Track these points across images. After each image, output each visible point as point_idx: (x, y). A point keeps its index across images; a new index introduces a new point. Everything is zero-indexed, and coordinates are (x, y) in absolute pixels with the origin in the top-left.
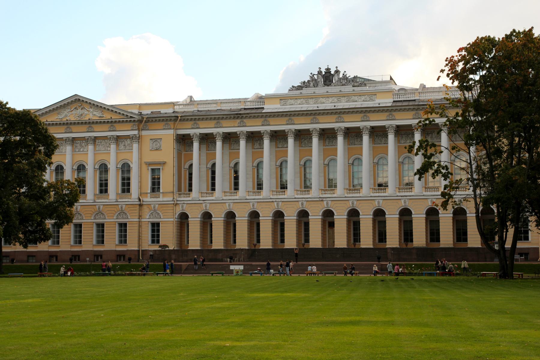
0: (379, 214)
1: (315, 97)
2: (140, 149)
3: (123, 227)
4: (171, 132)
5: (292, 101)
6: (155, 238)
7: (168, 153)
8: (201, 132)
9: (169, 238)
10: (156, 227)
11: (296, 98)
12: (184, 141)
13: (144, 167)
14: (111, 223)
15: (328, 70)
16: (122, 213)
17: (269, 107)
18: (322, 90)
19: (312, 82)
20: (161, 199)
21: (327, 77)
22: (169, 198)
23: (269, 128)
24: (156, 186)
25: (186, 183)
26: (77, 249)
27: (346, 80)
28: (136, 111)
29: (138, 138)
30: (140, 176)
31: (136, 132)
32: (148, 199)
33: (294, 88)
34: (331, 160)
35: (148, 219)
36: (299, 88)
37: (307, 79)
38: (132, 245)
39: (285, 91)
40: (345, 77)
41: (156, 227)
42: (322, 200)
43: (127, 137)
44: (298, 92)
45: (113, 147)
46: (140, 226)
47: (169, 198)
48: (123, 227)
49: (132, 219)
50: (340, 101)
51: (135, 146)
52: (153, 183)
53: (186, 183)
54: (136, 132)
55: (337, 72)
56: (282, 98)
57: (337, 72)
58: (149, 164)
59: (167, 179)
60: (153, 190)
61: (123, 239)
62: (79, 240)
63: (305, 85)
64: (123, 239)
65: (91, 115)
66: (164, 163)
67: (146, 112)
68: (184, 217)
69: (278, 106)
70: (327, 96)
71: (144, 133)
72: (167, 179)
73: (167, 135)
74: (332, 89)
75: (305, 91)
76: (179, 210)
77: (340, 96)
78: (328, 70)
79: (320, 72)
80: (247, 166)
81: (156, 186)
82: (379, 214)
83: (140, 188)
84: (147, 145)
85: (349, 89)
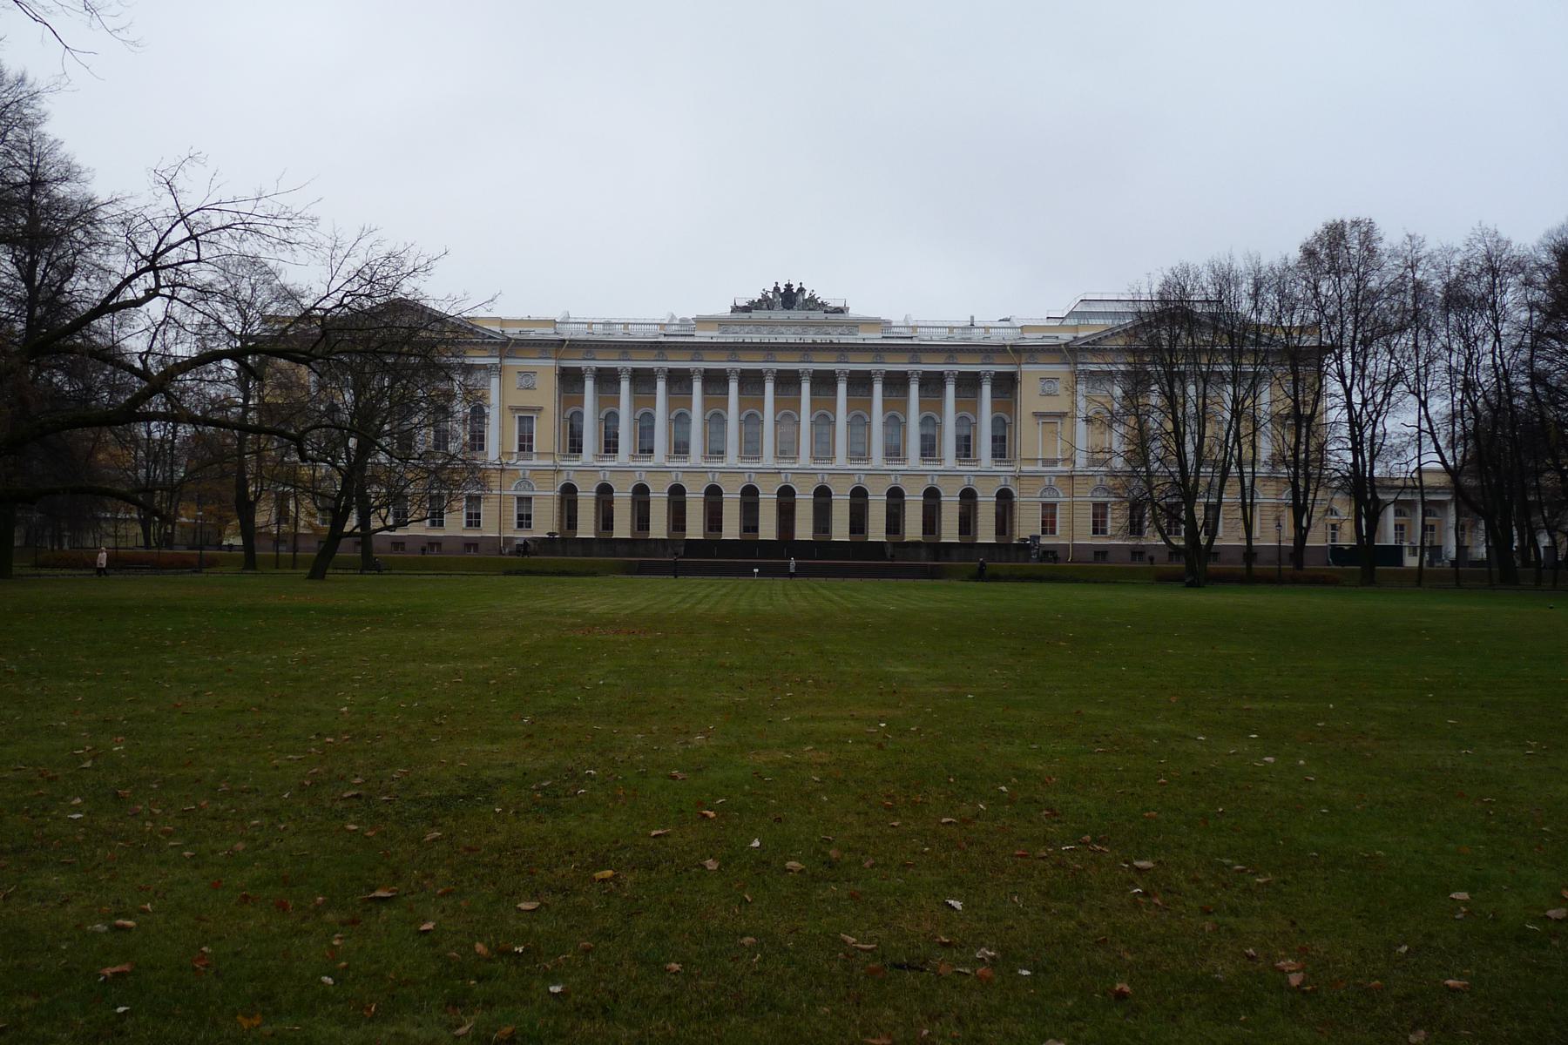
0: (859, 494)
1: (771, 324)
4: (552, 363)
5: (737, 329)
6: (524, 521)
7: (546, 393)
8: (593, 368)
11: (742, 324)
12: (570, 380)
13: (508, 412)
15: (789, 286)
17: (703, 336)
18: (780, 315)
19: (764, 303)
20: (535, 462)
21: (789, 297)
24: (526, 444)
26: (472, 534)
27: (813, 304)
28: (497, 329)
29: (499, 370)
30: (502, 427)
31: (496, 361)
33: (735, 309)
34: (680, 414)
35: (512, 491)
36: (746, 309)
37: (757, 296)
39: (724, 310)
40: (812, 299)
42: (779, 472)
43: (484, 367)
44: (746, 315)
50: (805, 333)
51: (495, 382)
52: (521, 439)
54: (496, 361)
55: (801, 290)
56: (720, 323)
57: (801, 290)
58: (518, 409)
60: (521, 448)
61: (1048, 525)
62: (474, 520)
66: (540, 409)
67: (512, 332)
68: (569, 491)
69: (715, 334)
70: (789, 324)
71: (508, 362)
72: (546, 433)
73: (546, 368)
74: (796, 315)
75: (755, 315)
76: (562, 480)
77: (807, 325)
78: (789, 286)
79: (777, 289)
81: (526, 444)
82: (859, 494)
83: (502, 444)
84: (514, 380)
85: (818, 315)
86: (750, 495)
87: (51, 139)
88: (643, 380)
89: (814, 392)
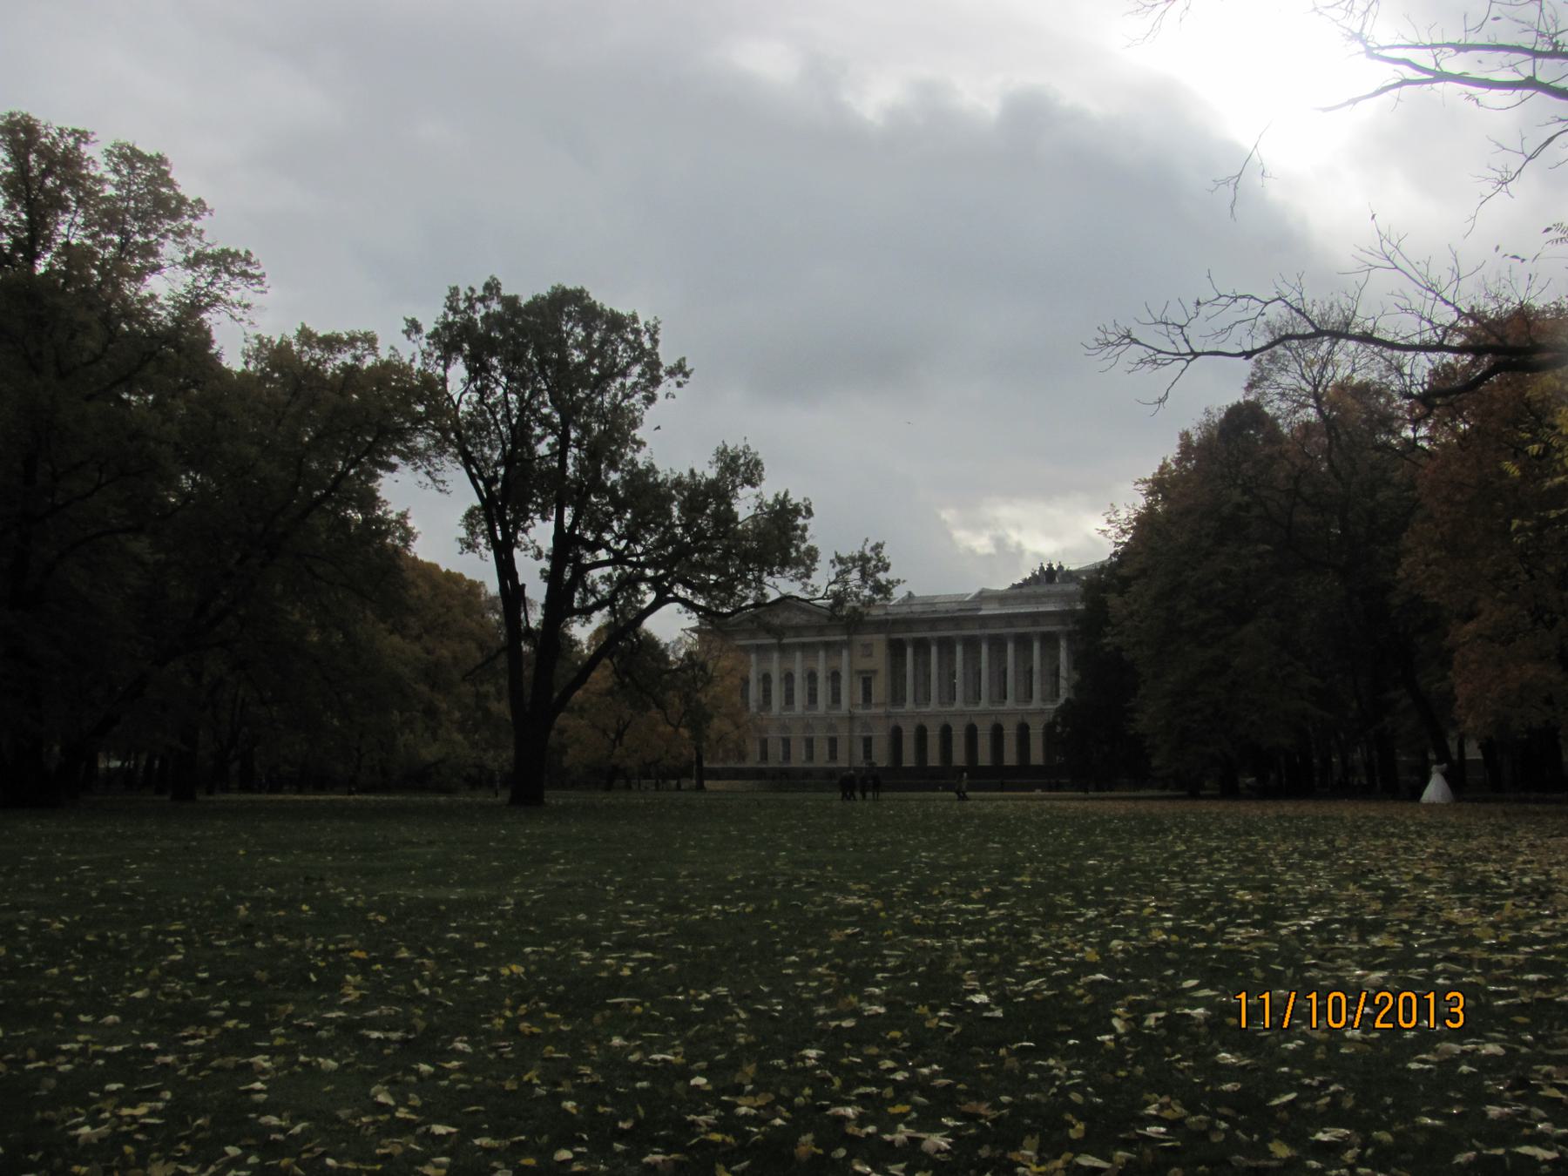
2: (850, 655)
3: (833, 742)
4: (882, 636)
7: (879, 660)
9: (881, 759)
10: (868, 742)
12: (897, 648)
14: (820, 735)
16: (831, 727)
17: (987, 610)
18: (1042, 589)
22: (880, 711)
23: (1013, 630)
25: (897, 697)
29: (847, 644)
32: (859, 711)
35: (858, 732)
36: (1020, 586)
38: (842, 762)
41: (868, 742)
43: (835, 643)
45: (822, 654)
46: (851, 742)
47: (880, 711)
48: (833, 742)
49: (842, 732)
51: (845, 653)
53: (897, 697)
55: (1060, 567)
56: (1002, 598)
57: (1060, 567)
58: (860, 672)
59: (880, 688)
63: (1026, 582)
64: (833, 755)
65: (799, 619)
66: (875, 672)
71: (855, 637)
72: (880, 688)
73: (879, 642)
74: (1053, 588)
75: (1025, 590)
80: (991, 673)
83: (851, 698)
86: (997, 732)
87: (686, 474)
88: (946, 645)
89: (915, 654)
